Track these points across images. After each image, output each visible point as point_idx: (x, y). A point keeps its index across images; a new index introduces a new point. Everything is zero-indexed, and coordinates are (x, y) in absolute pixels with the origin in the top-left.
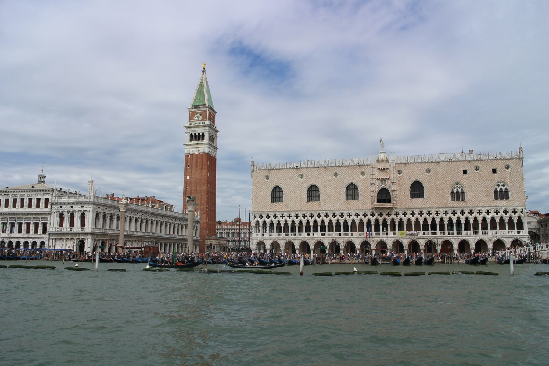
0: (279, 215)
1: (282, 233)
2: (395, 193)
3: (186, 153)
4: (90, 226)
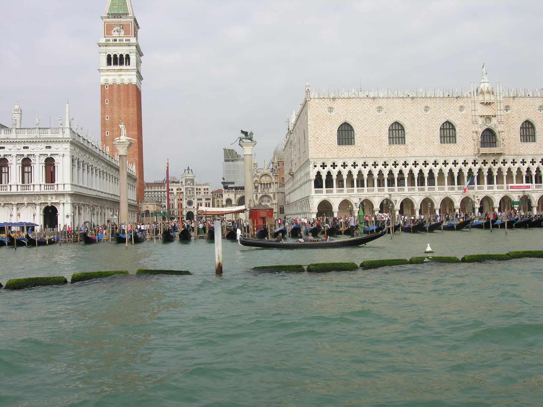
0: (350, 163)
1: (355, 188)
2: (503, 135)
3: (103, 82)
4: (68, 180)
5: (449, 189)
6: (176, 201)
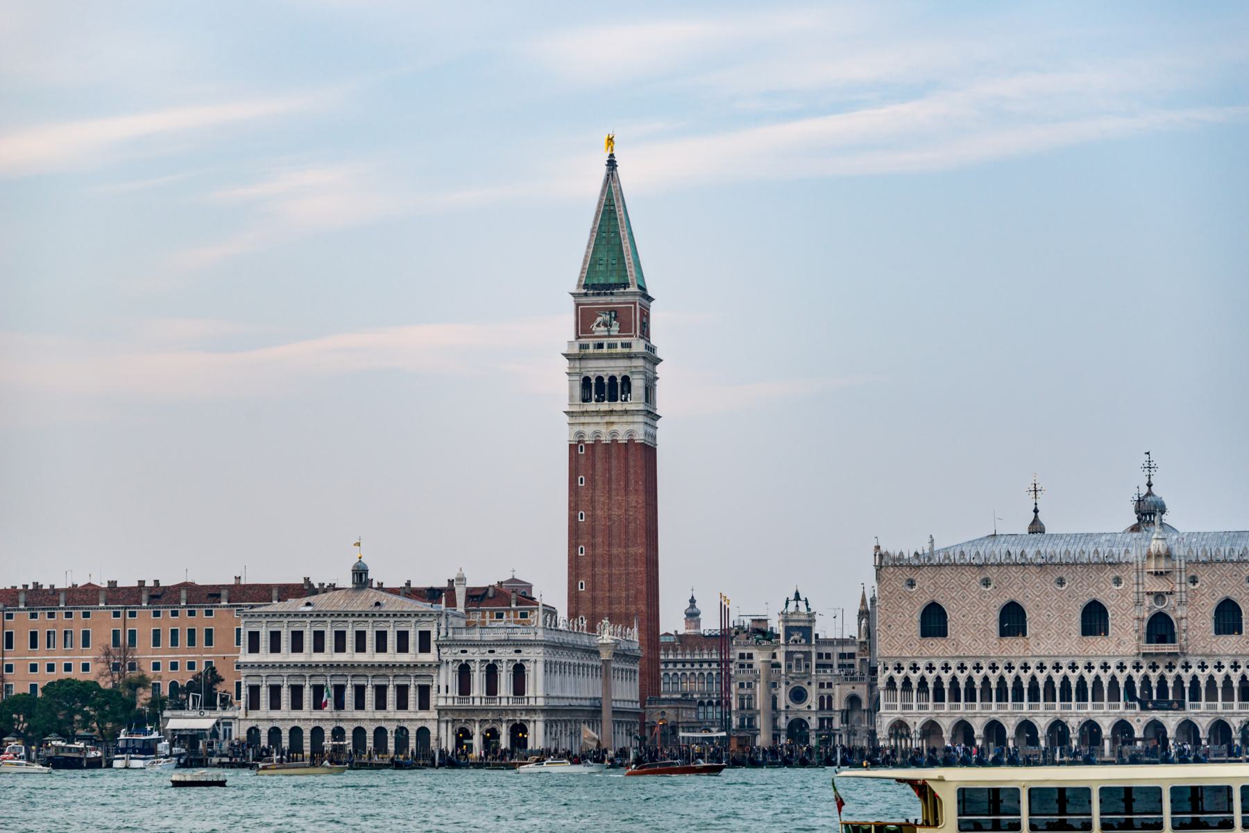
0: (938, 664)
2: (1184, 624)
4: (540, 693)
5: (1095, 707)
6: (760, 689)
